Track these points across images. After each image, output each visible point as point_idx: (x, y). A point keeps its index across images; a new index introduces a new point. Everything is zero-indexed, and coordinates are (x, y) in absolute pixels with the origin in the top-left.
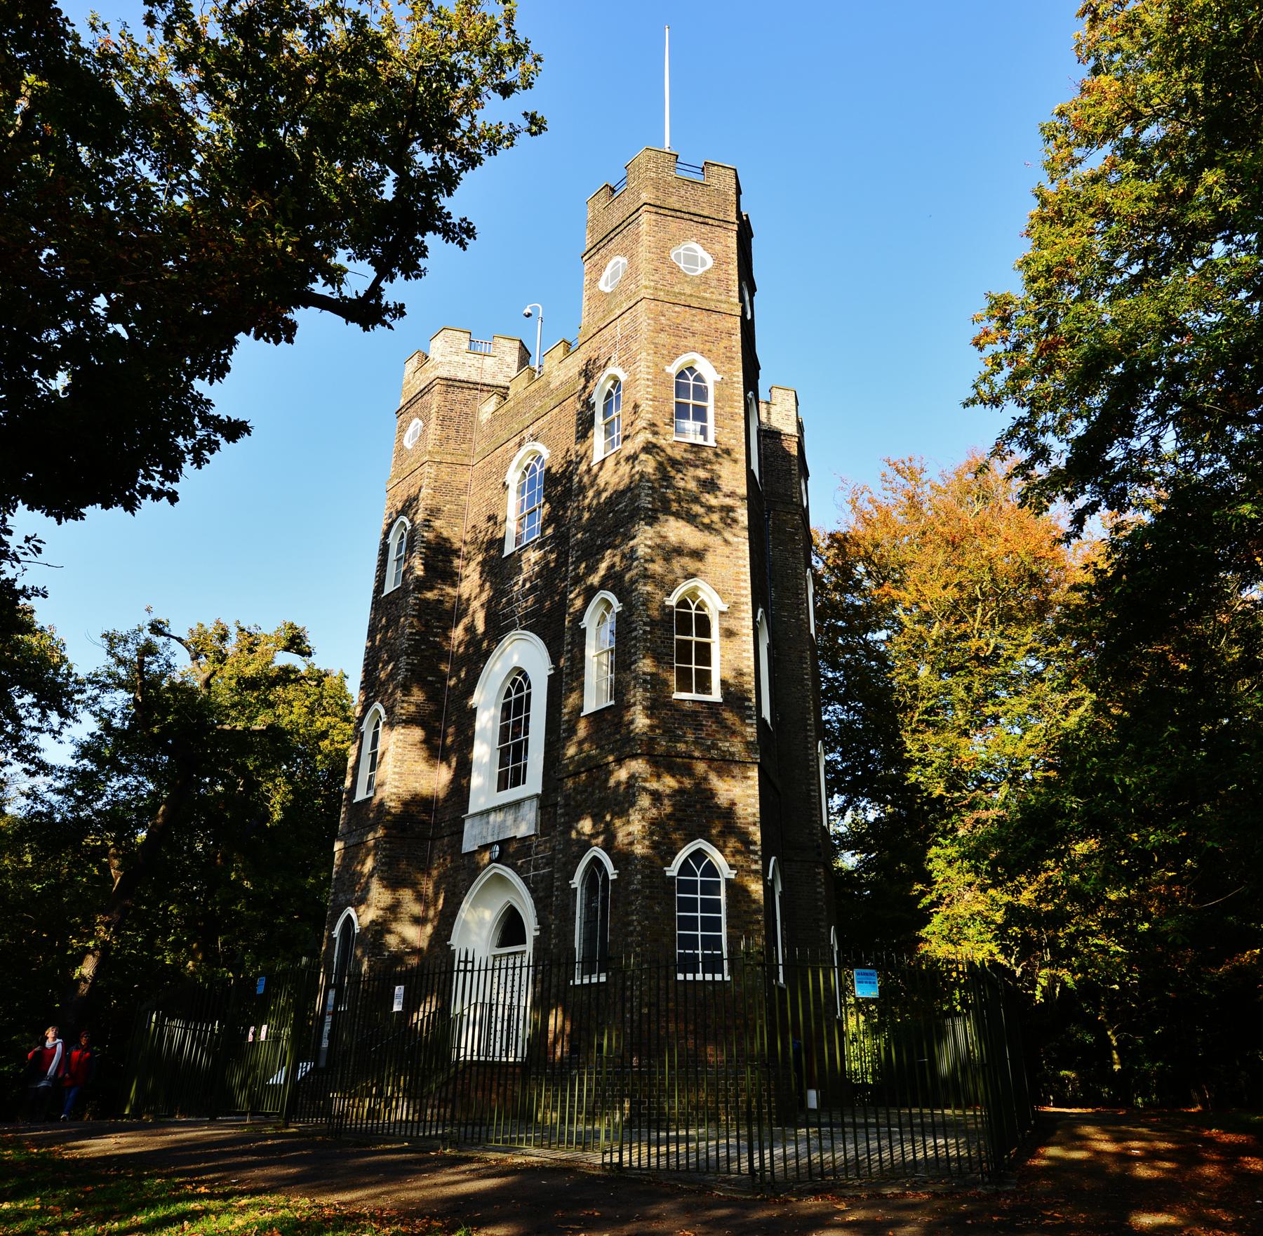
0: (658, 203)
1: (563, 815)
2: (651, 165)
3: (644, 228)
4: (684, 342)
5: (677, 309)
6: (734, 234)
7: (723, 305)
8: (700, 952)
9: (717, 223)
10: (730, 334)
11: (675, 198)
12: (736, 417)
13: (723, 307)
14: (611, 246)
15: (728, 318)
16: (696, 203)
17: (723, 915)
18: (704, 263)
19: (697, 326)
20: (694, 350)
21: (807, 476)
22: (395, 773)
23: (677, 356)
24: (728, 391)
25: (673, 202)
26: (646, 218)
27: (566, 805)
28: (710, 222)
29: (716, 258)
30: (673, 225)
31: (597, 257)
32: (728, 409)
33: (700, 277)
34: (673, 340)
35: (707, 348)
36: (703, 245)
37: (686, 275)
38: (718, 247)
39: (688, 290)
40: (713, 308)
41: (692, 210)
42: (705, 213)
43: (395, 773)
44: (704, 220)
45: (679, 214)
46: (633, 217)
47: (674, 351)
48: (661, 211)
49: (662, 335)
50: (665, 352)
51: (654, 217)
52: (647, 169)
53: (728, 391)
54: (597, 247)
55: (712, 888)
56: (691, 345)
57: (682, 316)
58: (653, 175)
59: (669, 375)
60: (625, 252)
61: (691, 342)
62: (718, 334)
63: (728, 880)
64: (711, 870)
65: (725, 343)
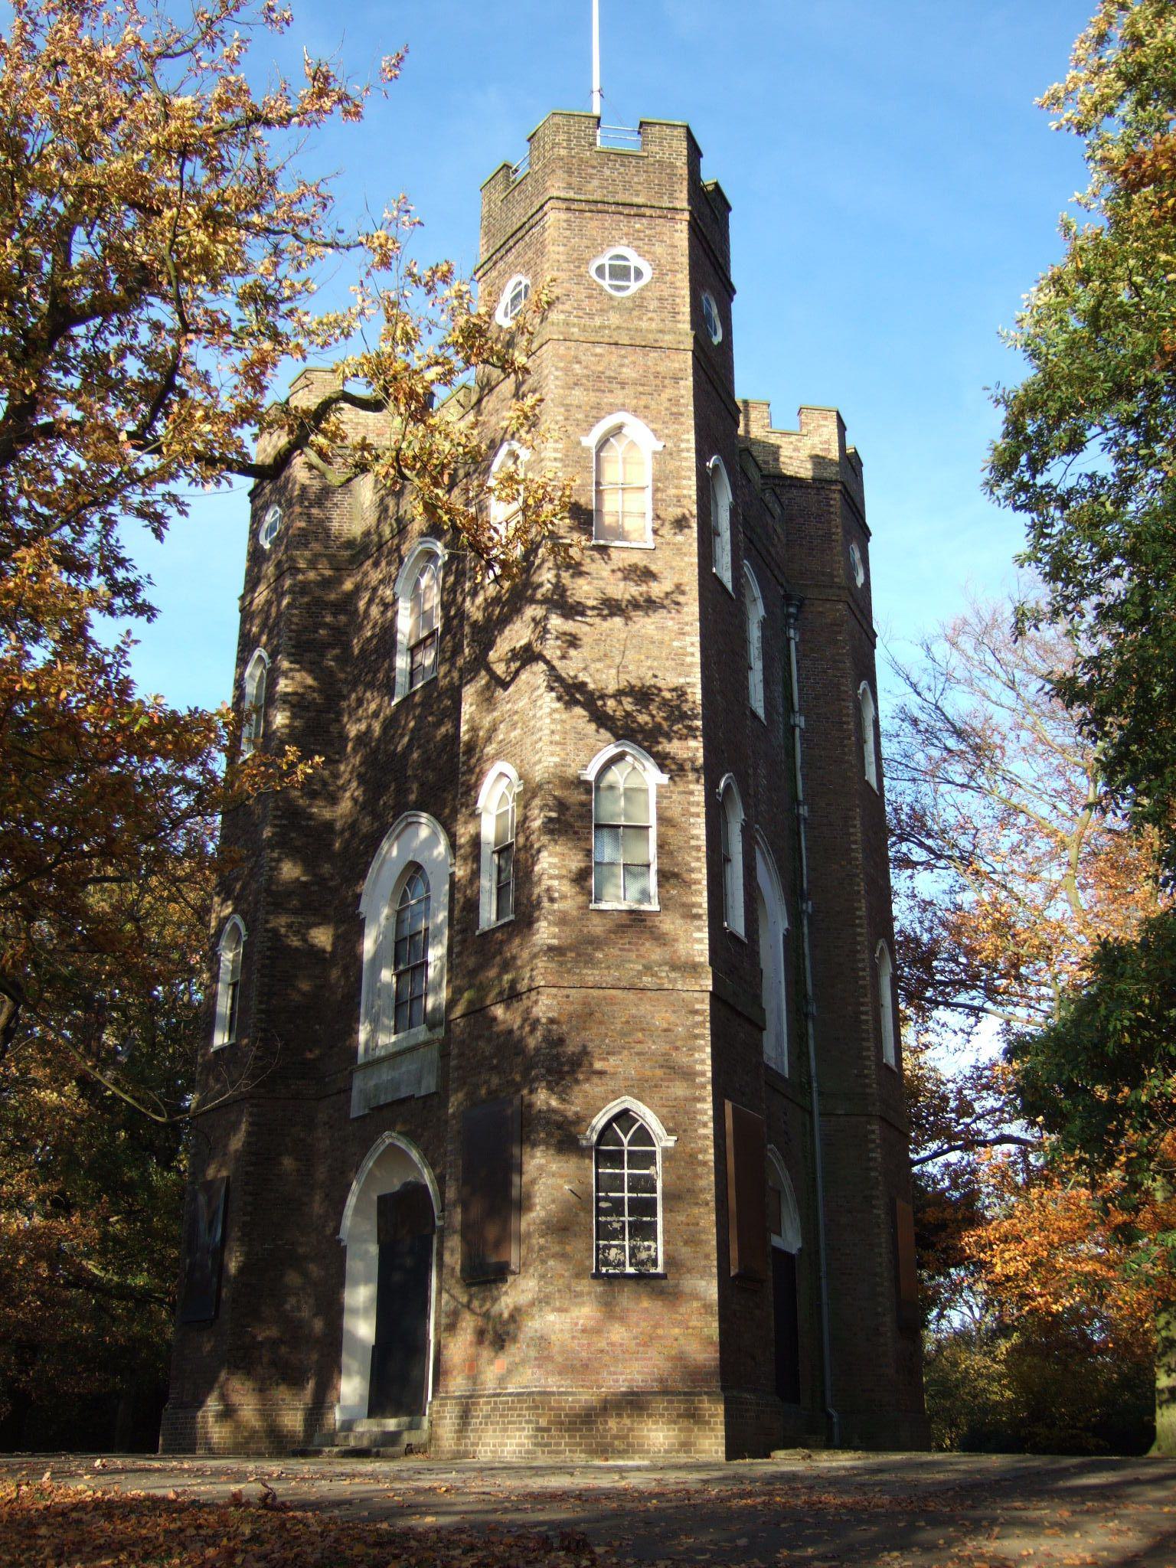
0: (571, 195)
1: (459, 1068)
2: (561, 137)
3: (550, 233)
4: (608, 399)
5: (598, 350)
6: (684, 226)
7: (667, 337)
8: (626, 1243)
9: (659, 212)
10: (676, 379)
11: (595, 183)
12: (685, 502)
13: (668, 339)
14: (510, 257)
15: (673, 355)
16: (627, 186)
17: (659, 1195)
18: (639, 274)
19: (628, 373)
20: (623, 407)
21: (865, 534)
22: (261, 1011)
23: (598, 419)
24: (672, 465)
25: (594, 190)
26: (554, 217)
27: (461, 1055)
28: (648, 212)
29: (657, 265)
30: (593, 225)
31: (494, 274)
32: (672, 491)
33: (633, 298)
34: (593, 398)
35: (642, 403)
36: (637, 248)
37: (611, 298)
38: (659, 249)
39: (614, 319)
40: (651, 343)
41: (620, 198)
42: (640, 200)
43: (261, 1011)
44: (636, 211)
45: (600, 206)
46: (537, 217)
47: (594, 413)
48: (574, 206)
49: (577, 392)
50: (580, 416)
51: (563, 216)
52: (554, 145)
53: (672, 465)
54: (492, 261)
55: (649, 1159)
56: (619, 401)
57: (606, 360)
58: (563, 152)
59: (587, 450)
60: (528, 267)
61: (619, 396)
62: (658, 382)
63: (665, 1150)
64: (643, 1136)
65: (669, 393)
